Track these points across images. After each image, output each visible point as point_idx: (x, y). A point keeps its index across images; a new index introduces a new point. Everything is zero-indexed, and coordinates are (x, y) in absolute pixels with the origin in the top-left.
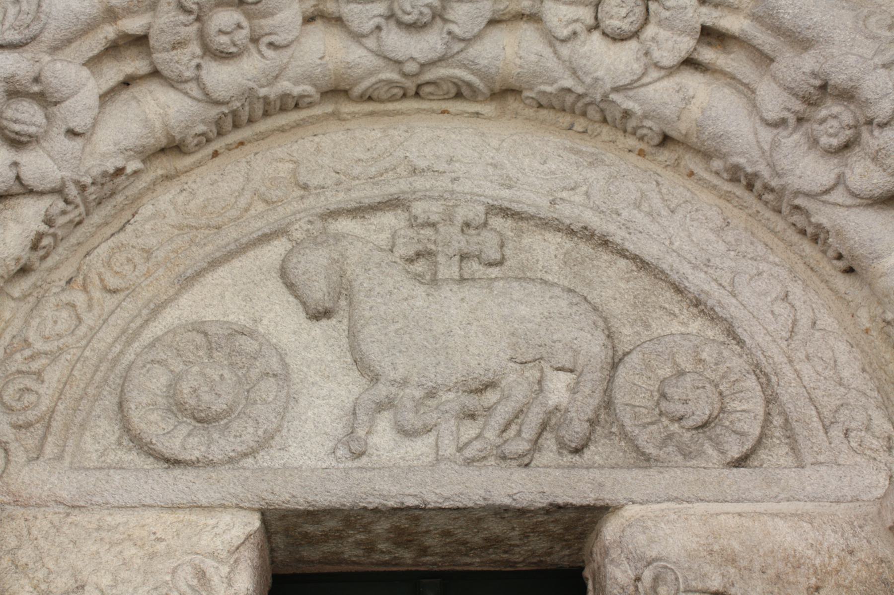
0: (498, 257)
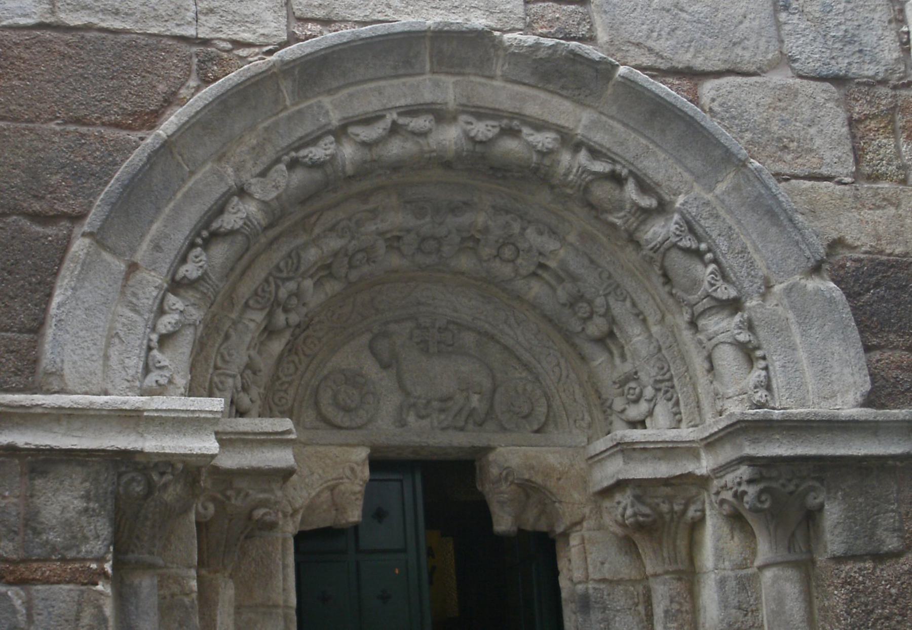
0: (452, 343)
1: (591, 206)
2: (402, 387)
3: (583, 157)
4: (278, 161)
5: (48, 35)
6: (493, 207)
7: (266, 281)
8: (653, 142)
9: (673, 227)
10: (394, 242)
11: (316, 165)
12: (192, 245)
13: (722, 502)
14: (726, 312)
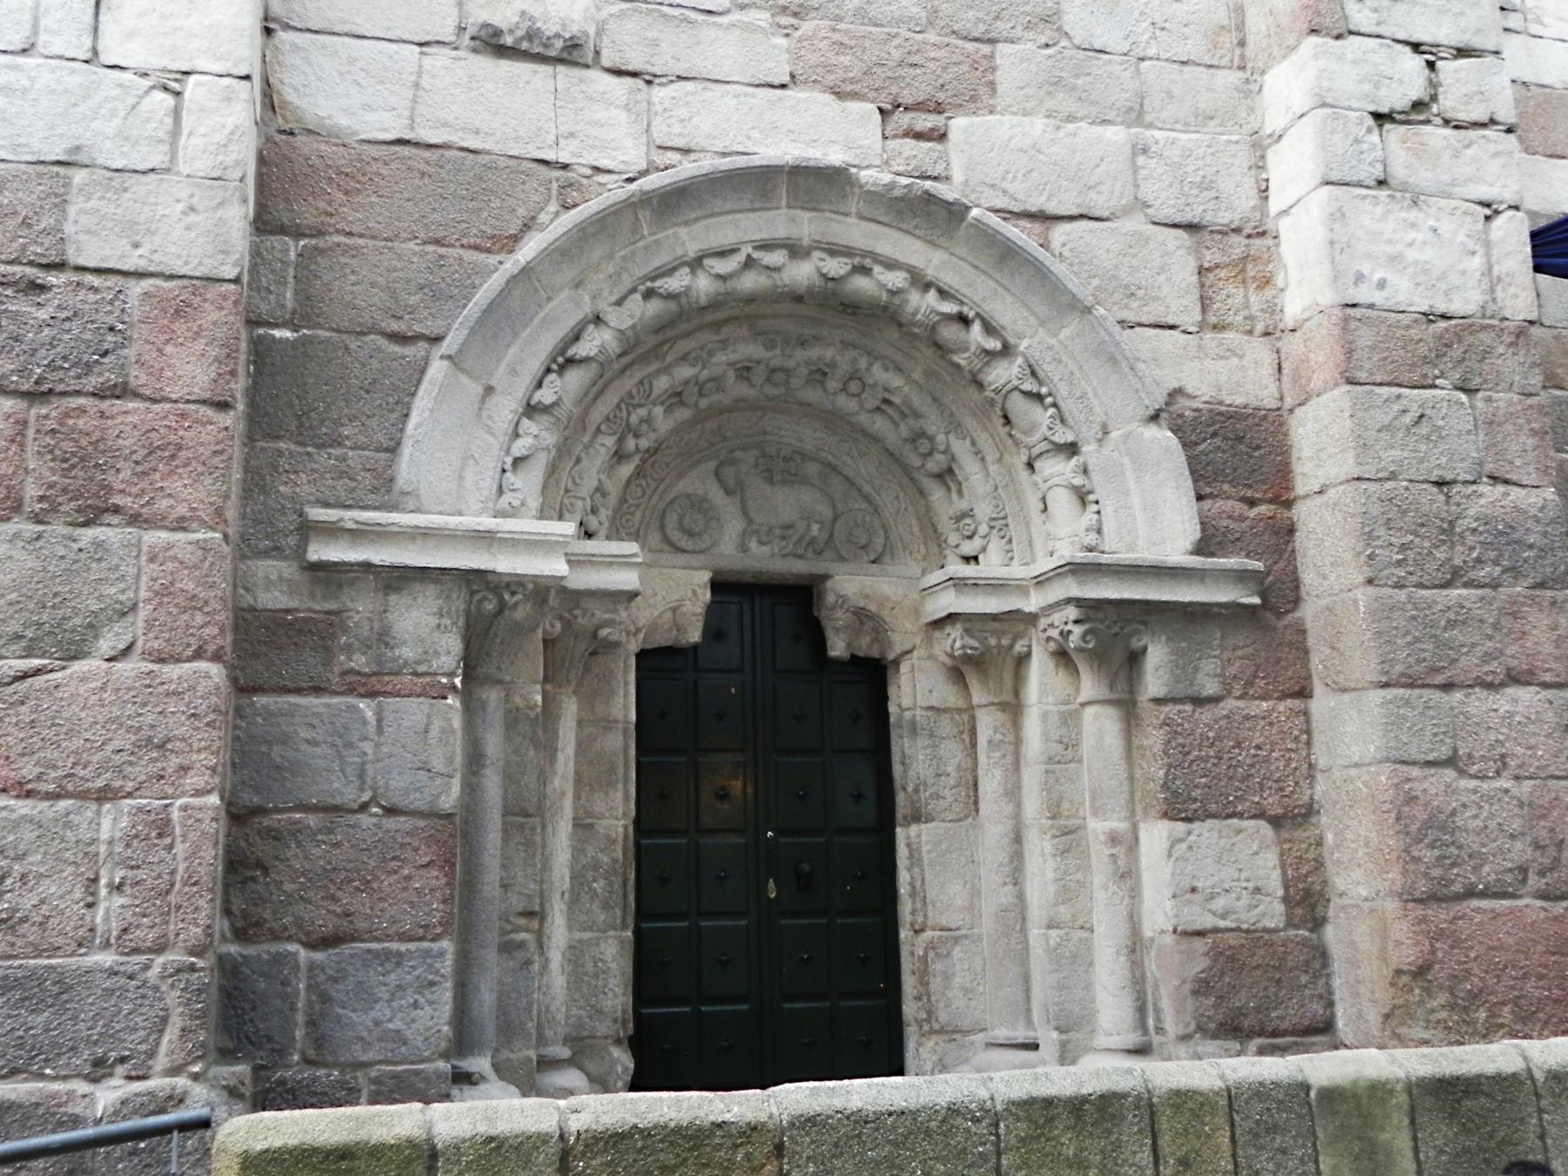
1: (937, 346)
2: (745, 513)
3: (932, 296)
4: (634, 290)
5: (406, 151)
6: (842, 342)
7: (618, 406)
8: (1001, 284)
9: (1015, 370)
10: (745, 371)
11: (670, 297)
12: (548, 371)
13: (1049, 639)
14: (1062, 456)
